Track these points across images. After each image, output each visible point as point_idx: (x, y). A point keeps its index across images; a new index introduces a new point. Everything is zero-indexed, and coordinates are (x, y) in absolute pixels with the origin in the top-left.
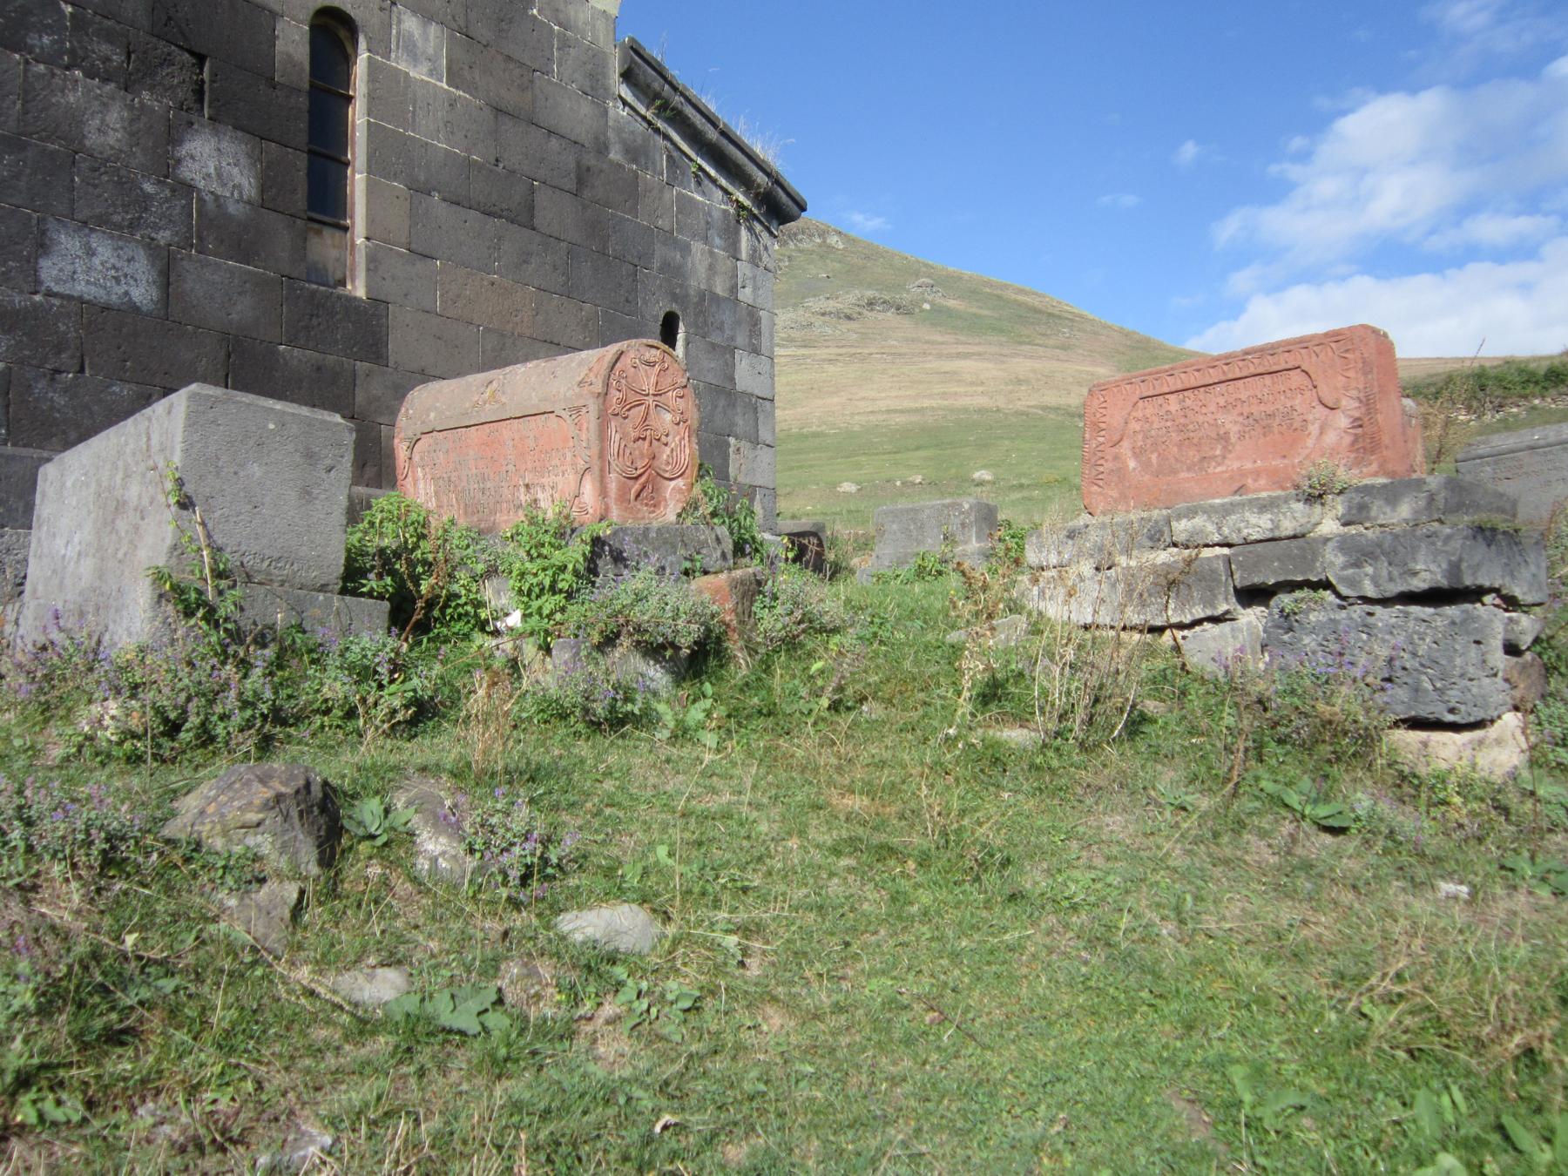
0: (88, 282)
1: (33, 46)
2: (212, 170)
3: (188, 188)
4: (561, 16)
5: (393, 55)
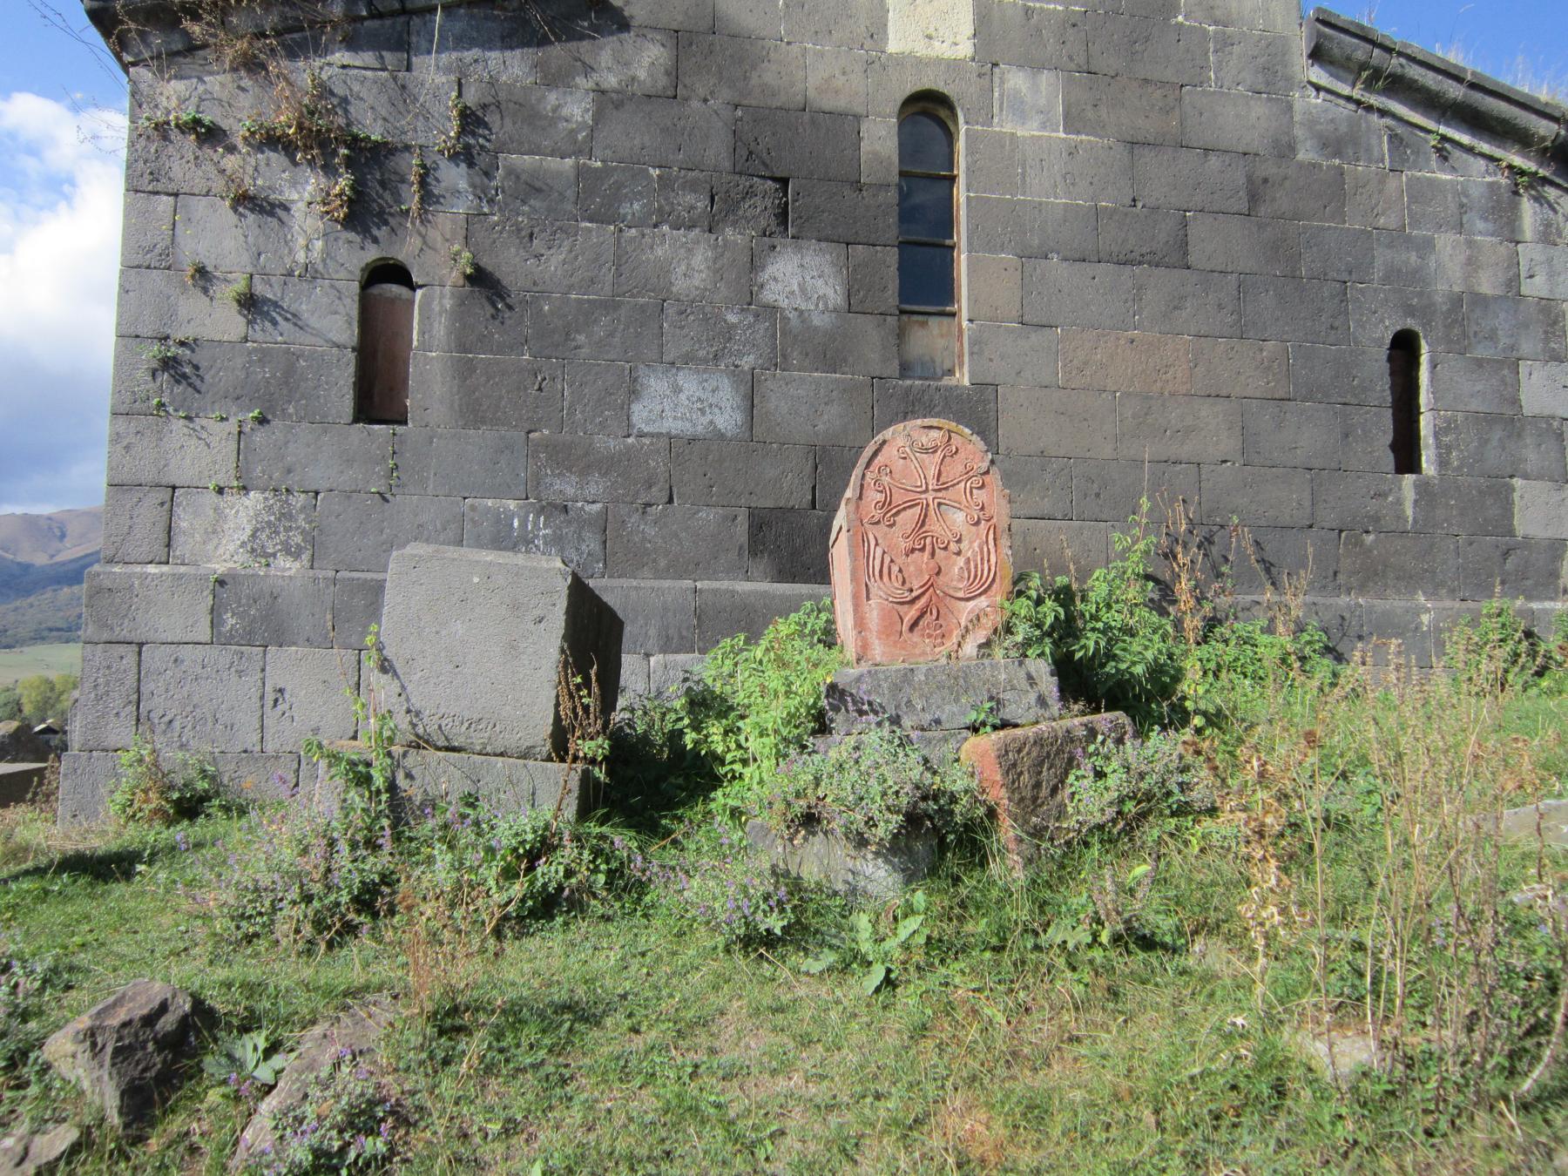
0: (675, 418)
1: (625, 215)
2: (795, 287)
3: (773, 309)
4: (1218, 13)
5: (996, 120)
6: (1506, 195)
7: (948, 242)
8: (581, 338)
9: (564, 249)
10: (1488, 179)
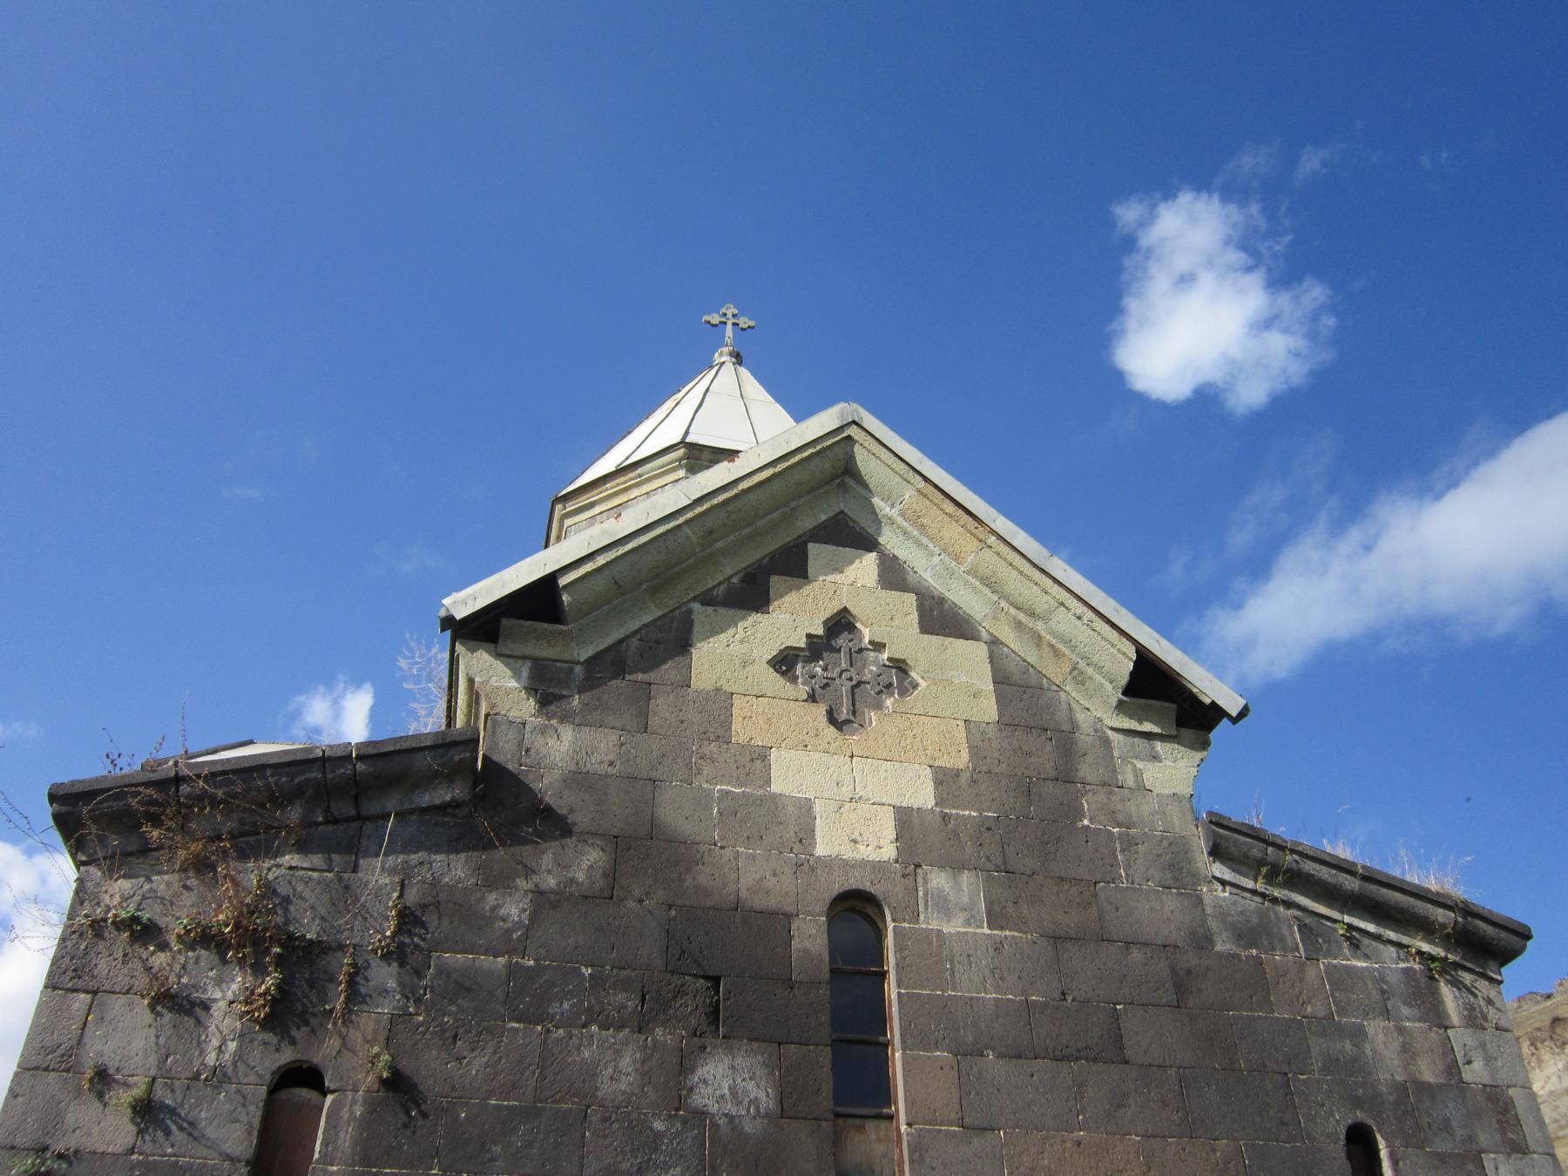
2: (726, 1091)
3: (702, 1114)
4: (1120, 817)
5: (922, 917)
6: (1423, 981)
7: (881, 1039)
8: (497, 1149)
9: (489, 1051)
10: (1402, 965)
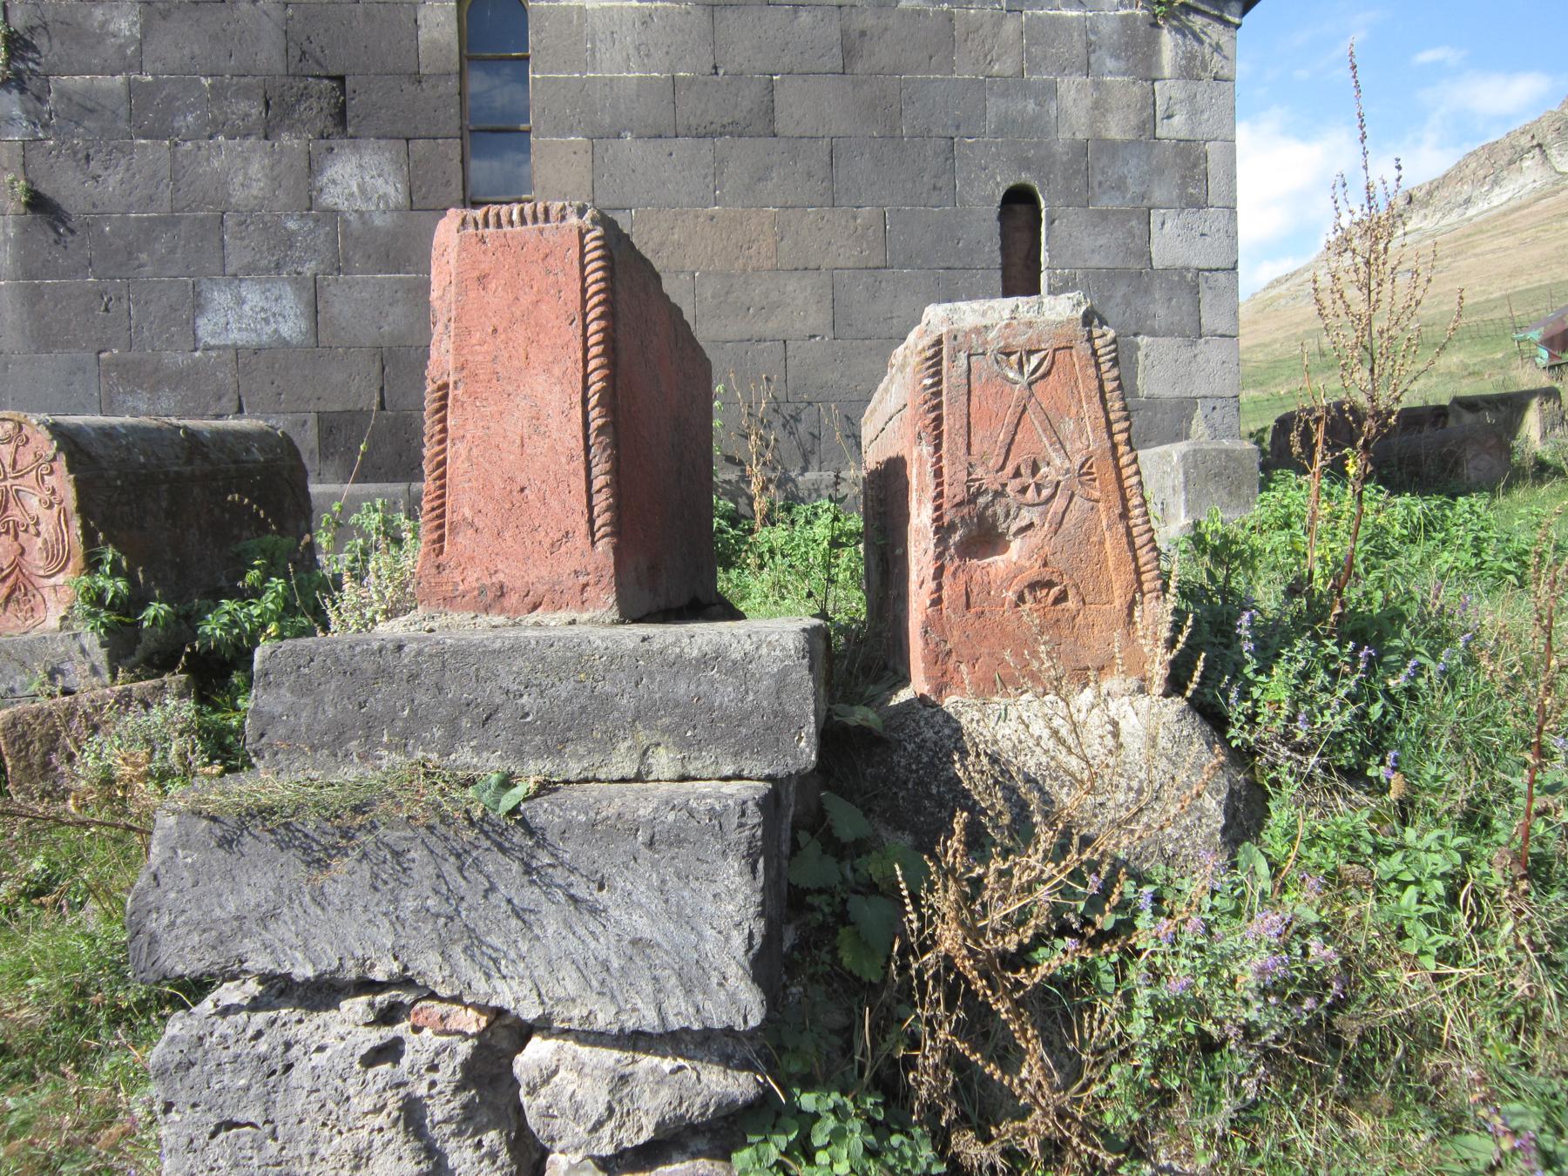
0: (240, 329)
1: (179, 129)
2: (355, 189)
3: (334, 212)
6: (1143, 28)
7: (523, 126)
8: (144, 257)
9: (121, 169)
10: (1122, 12)
